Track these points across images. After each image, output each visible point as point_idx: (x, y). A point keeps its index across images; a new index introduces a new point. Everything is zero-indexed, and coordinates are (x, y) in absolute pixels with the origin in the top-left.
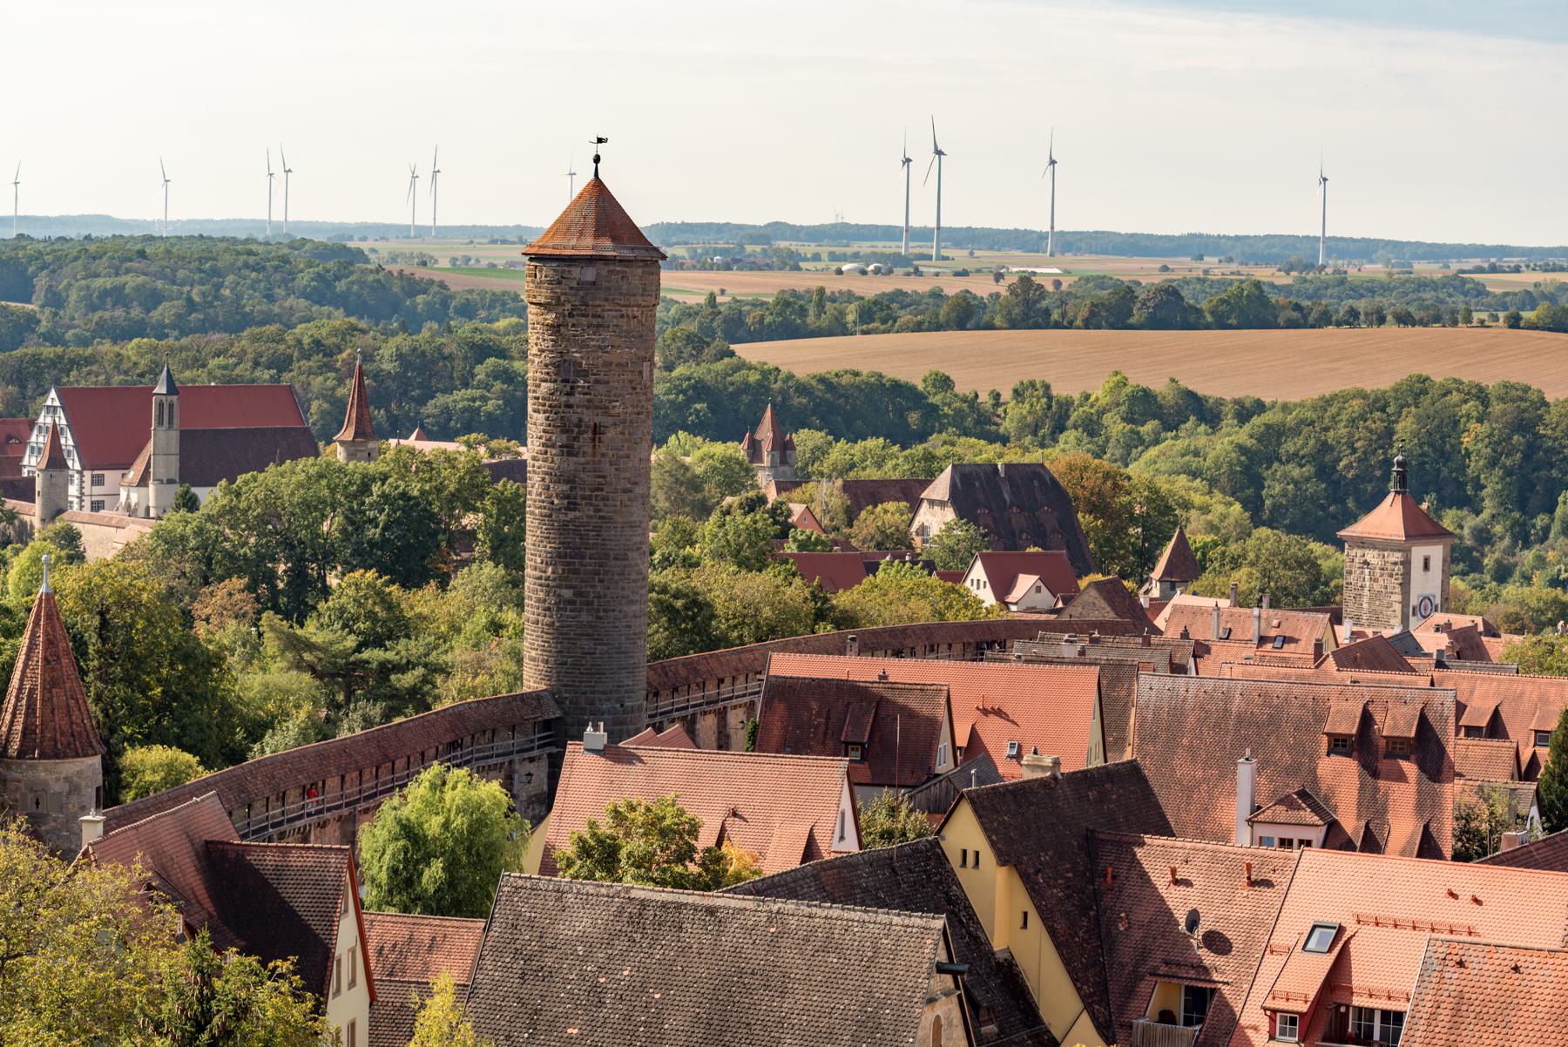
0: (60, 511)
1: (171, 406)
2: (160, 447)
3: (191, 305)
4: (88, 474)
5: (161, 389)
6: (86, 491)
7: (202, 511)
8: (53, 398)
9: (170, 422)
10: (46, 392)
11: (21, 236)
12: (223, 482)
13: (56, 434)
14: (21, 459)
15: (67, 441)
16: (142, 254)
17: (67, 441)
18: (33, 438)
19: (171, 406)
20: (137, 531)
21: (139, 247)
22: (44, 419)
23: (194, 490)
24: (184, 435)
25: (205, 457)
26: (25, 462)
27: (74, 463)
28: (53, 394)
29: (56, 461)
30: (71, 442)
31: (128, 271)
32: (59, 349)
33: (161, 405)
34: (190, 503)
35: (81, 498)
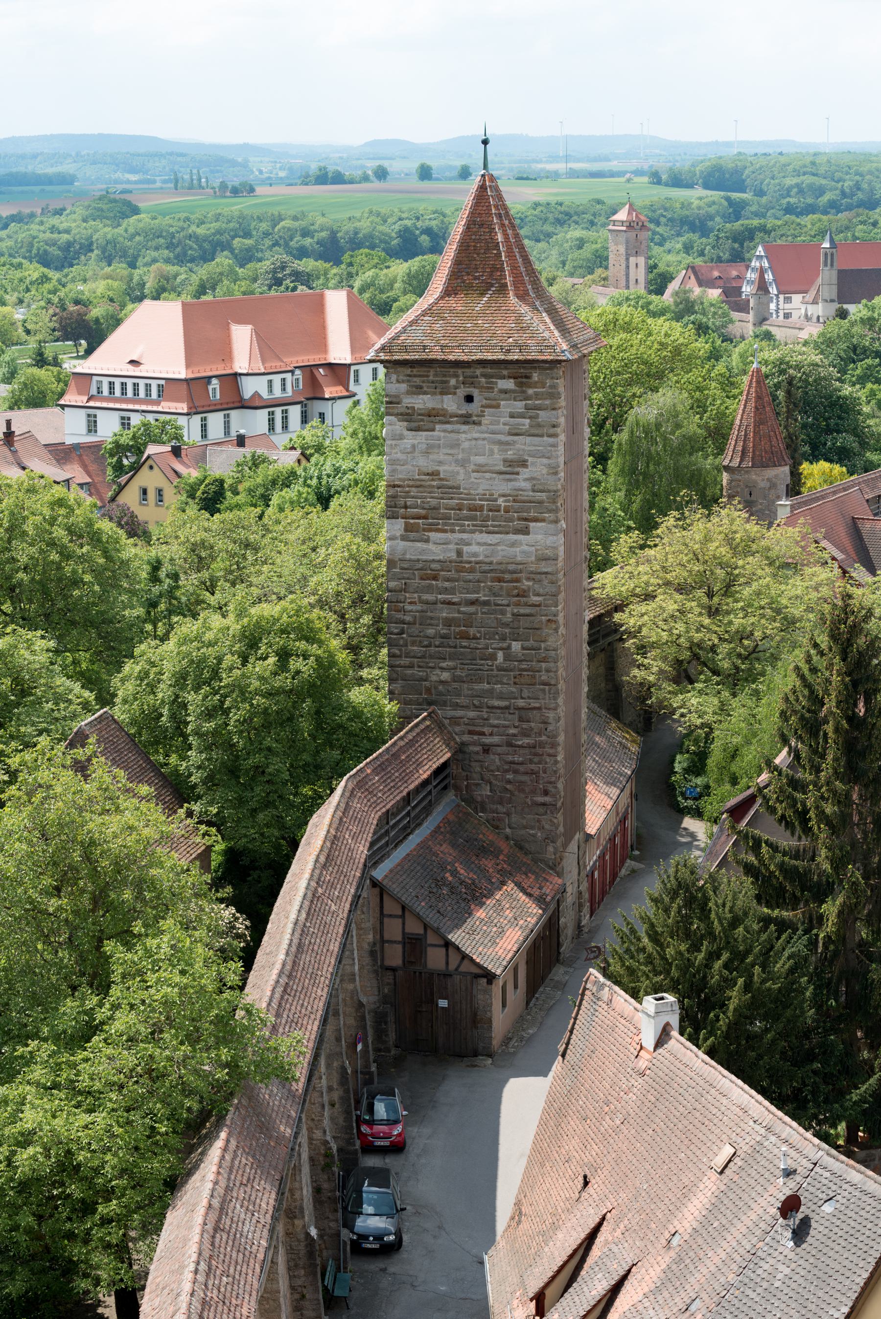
0: (765, 319)
1: (832, 255)
2: (826, 278)
3: (843, 194)
4: (781, 297)
5: (826, 245)
6: (781, 307)
7: (851, 317)
8: (760, 251)
9: (832, 265)
10: (755, 247)
11: (740, 153)
12: (864, 301)
13: (762, 272)
14: (741, 287)
15: (769, 277)
16: (813, 163)
17: (769, 277)
18: (748, 275)
19: (832, 255)
20: (812, 331)
21: (811, 159)
22: (755, 263)
23: (845, 306)
24: (842, 274)
25: (853, 285)
26: (744, 289)
27: (773, 290)
28: (760, 248)
29: (763, 287)
30: (771, 277)
31: (804, 174)
32: (762, 221)
33: (826, 254)
34: (843, 314)
35: (777, 311)
